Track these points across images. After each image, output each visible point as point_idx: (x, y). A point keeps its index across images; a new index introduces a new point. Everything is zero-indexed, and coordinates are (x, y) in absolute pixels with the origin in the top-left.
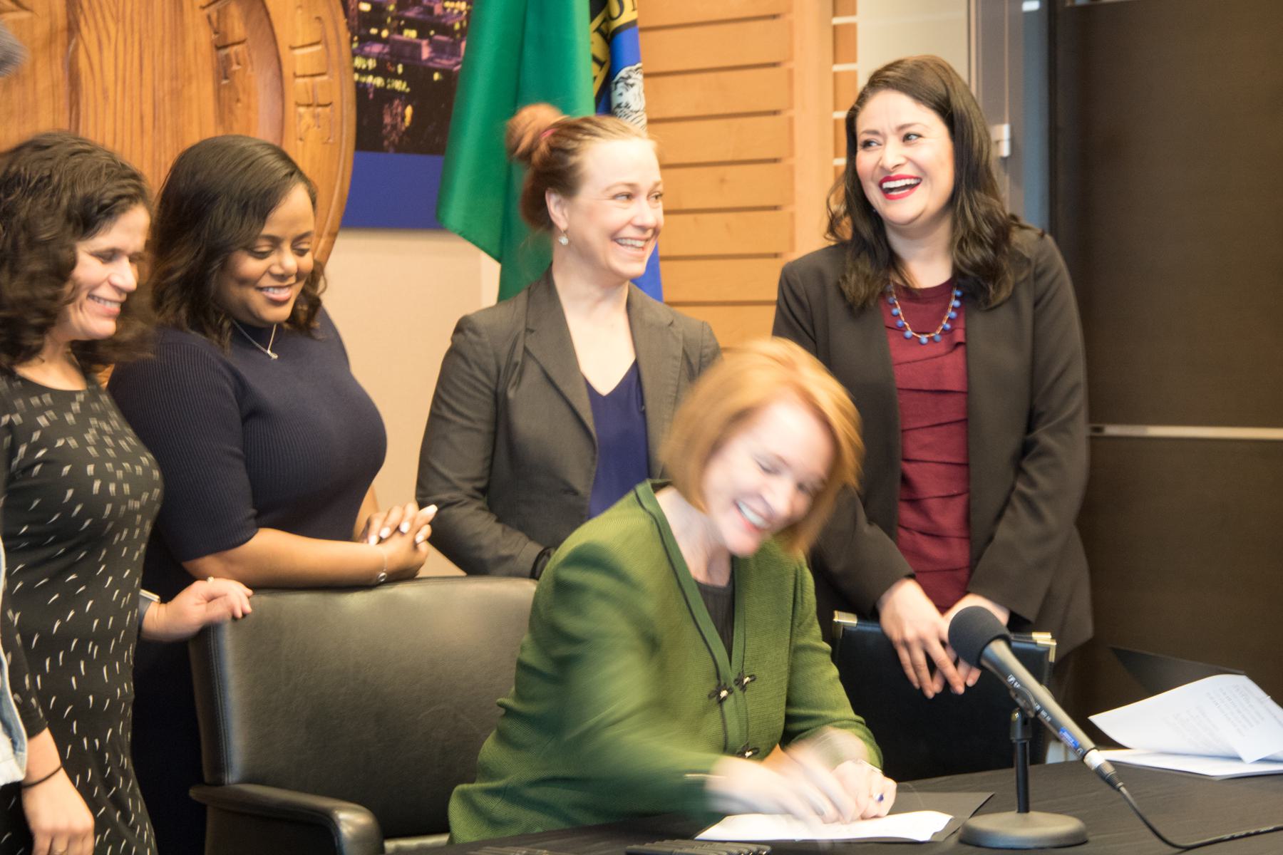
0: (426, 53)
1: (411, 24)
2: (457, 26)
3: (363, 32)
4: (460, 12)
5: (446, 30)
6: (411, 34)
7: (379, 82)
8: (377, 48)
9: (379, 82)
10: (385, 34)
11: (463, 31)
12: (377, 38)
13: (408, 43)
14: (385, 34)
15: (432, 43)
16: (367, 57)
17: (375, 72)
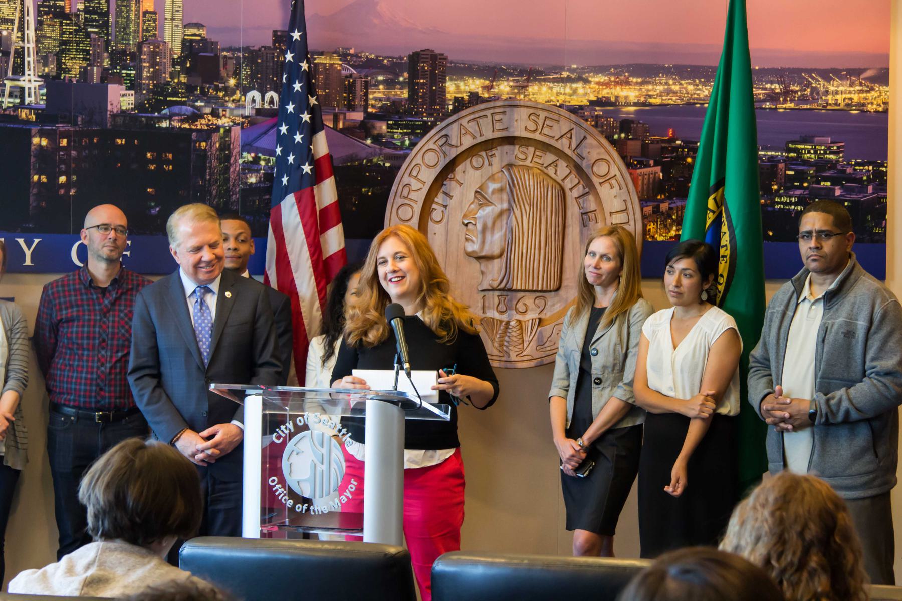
0: (838, 192)
1: (826, 179)
2: (865, 178)
3: (788, 185)
4: (869, 171)
5: (860, 181)
6: (829, 184)
7: (799, 208)
8: (798, 192)
9: (799, 208)
10: (805, 185)
11: (869, 181)
12: (801, 187)
13: (826, 188)
14: (805, 185)
15: (842, 187)
16: (790, 197)
17: (796, 204)
